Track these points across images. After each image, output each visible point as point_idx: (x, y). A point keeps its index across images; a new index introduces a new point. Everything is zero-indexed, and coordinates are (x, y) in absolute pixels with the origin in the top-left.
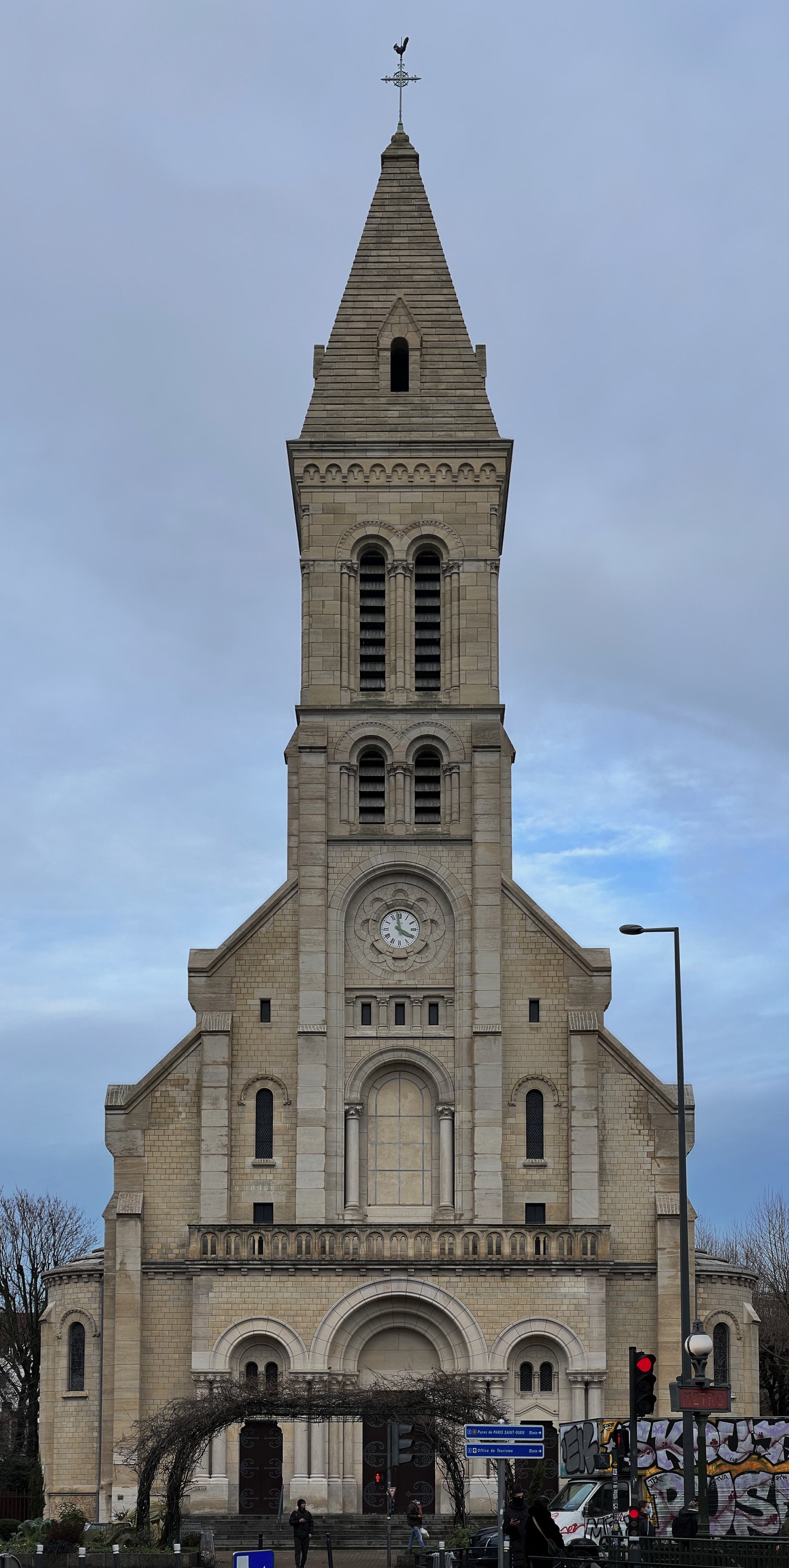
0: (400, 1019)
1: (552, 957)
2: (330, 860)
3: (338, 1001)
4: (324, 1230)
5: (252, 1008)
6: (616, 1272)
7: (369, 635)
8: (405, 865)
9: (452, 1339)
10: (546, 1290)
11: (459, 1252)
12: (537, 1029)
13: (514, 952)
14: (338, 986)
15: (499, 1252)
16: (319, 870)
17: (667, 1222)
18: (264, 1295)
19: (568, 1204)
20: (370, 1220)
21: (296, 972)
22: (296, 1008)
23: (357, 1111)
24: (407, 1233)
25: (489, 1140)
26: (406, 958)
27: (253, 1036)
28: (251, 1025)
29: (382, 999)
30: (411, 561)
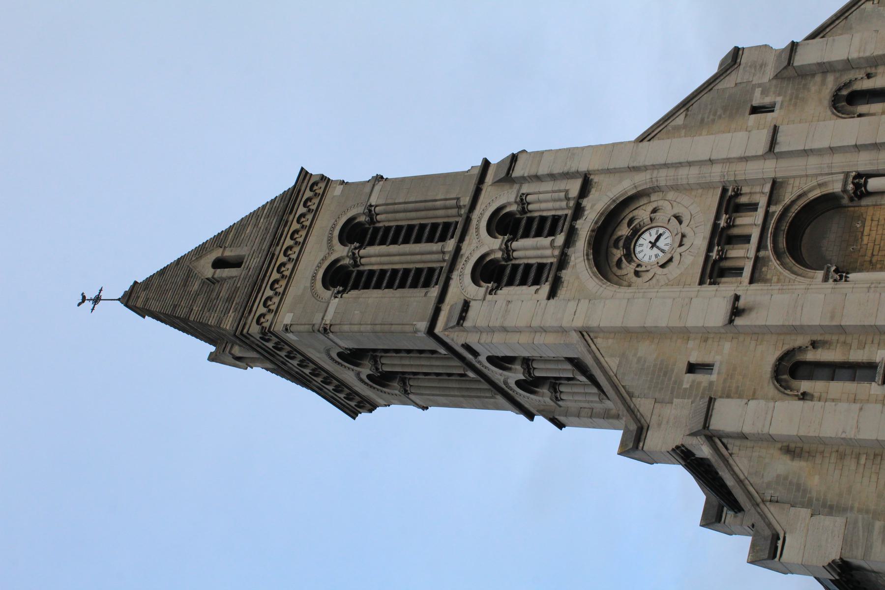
3: (708, 289)
29: (718, 254)
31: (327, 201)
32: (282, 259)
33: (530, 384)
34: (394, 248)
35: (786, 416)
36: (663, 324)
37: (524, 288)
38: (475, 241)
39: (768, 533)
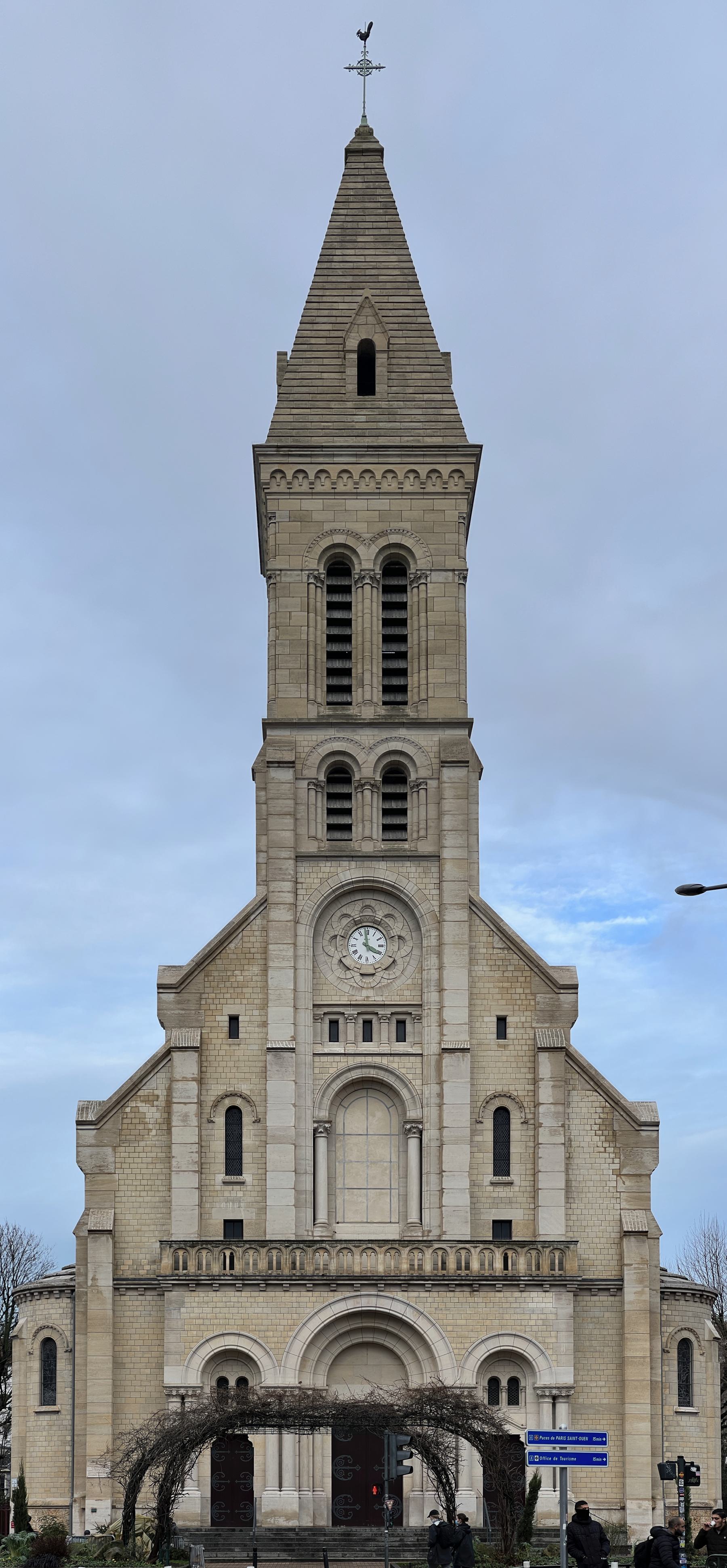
0: (368, 1037)
1: (520, 974)
2: (299, 875)
3: (306, 1017)
4: (295, 1246)
5: (221, 1024)
6: (584, 1287)
7: (336, 648)
8: (373, 881)
9: (421, 1353)
10: (514, 1305)
11: (428, 1268)
12: (505, 1046)
13: (481, 969)
14: (306, 1002)
15: (467, 1267)
16: (288, 886)
17: (632, 1239)
18: (235, 1310)
19: (535, 1220)
20: (338, 1237)
21: (265, 987)
22: (265, 1024)
23: (326, 1129)
24: (377, 1249)
25: (457, 1157)
26: (373, 975)
27: (222, 1053)
28: (220, 1041)
29: (350, 1015)
30: (378, 571)
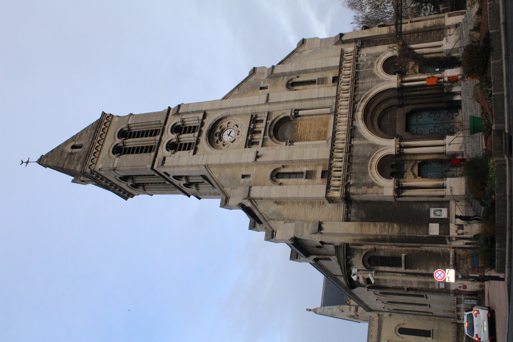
3: (248, 149)
31: (113, 123)
32: (97, 144)
33: (188, 185)
34: (138, 139)
35: (275, 191)
36: (233, 162)
37: (185, 151)
38: (167, 136)
39: (270, 230)
